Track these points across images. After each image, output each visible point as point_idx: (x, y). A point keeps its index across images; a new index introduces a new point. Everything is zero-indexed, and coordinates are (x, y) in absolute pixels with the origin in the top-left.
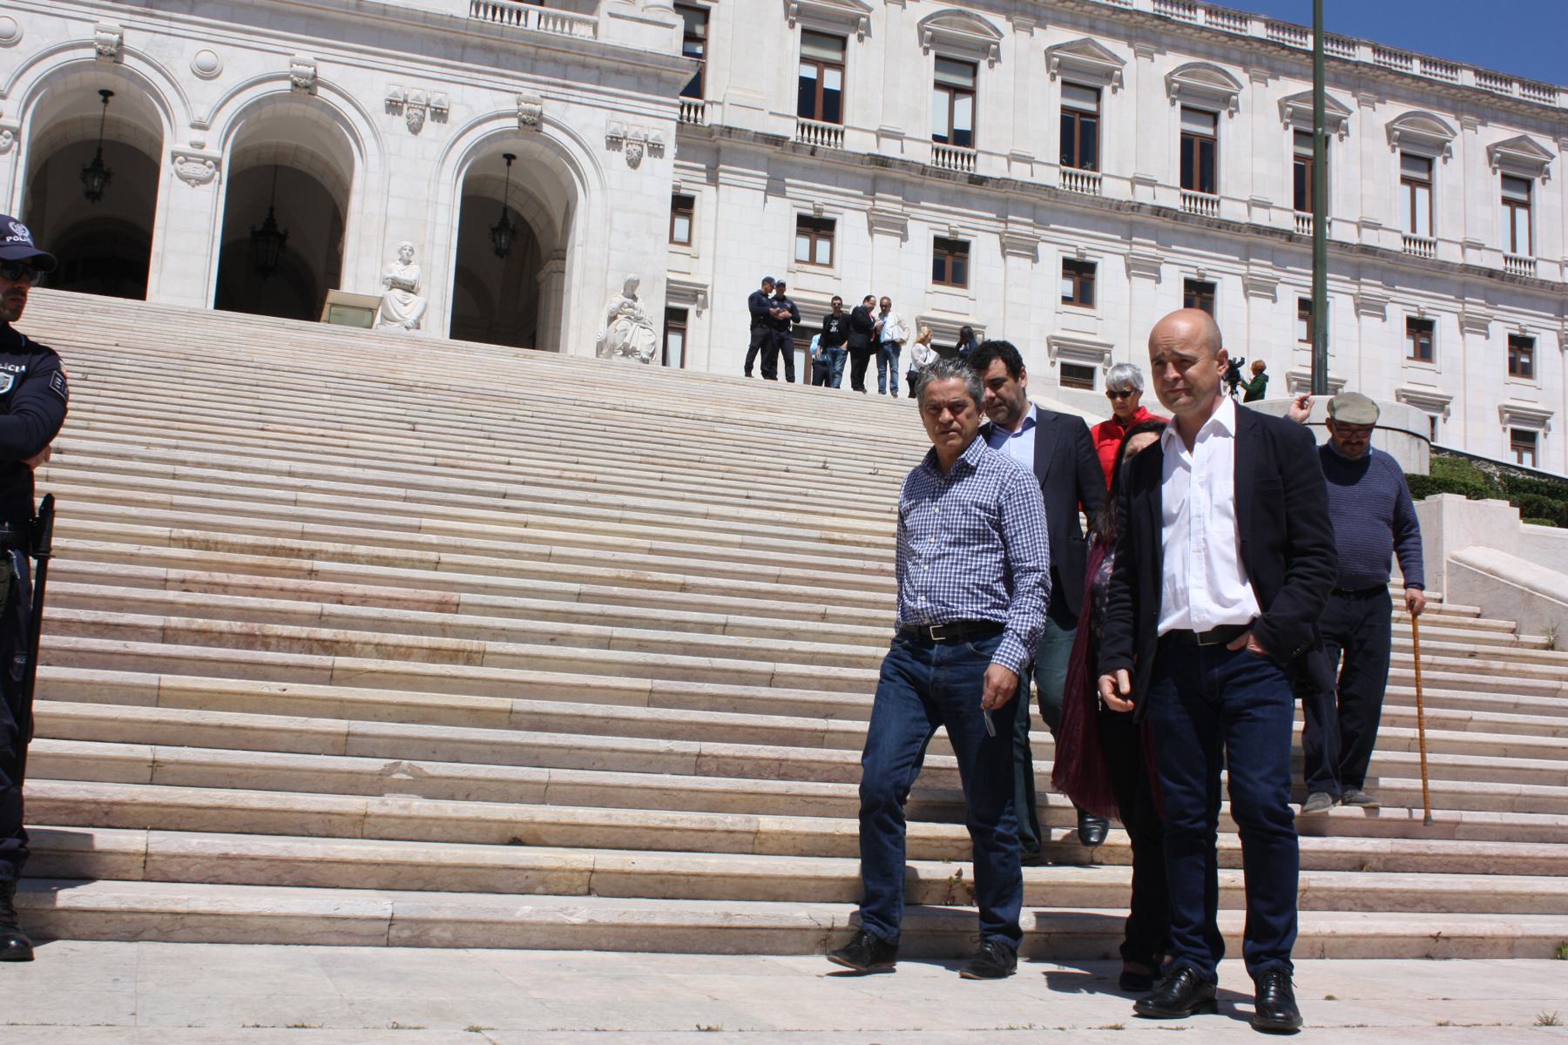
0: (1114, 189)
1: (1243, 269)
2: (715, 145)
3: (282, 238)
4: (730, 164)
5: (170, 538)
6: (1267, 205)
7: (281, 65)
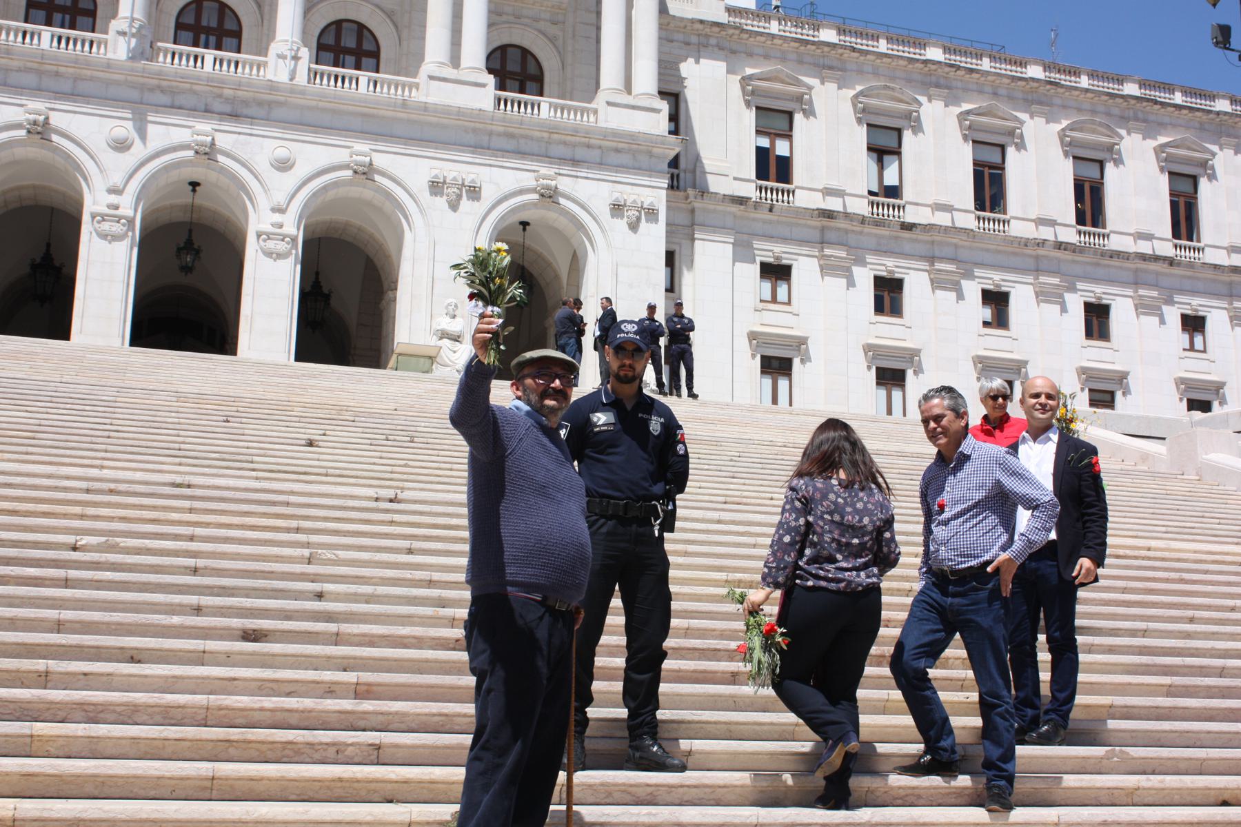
0: (1019, 229)
3: (327, 297)
5: (727, 581)
7: (342, 156)
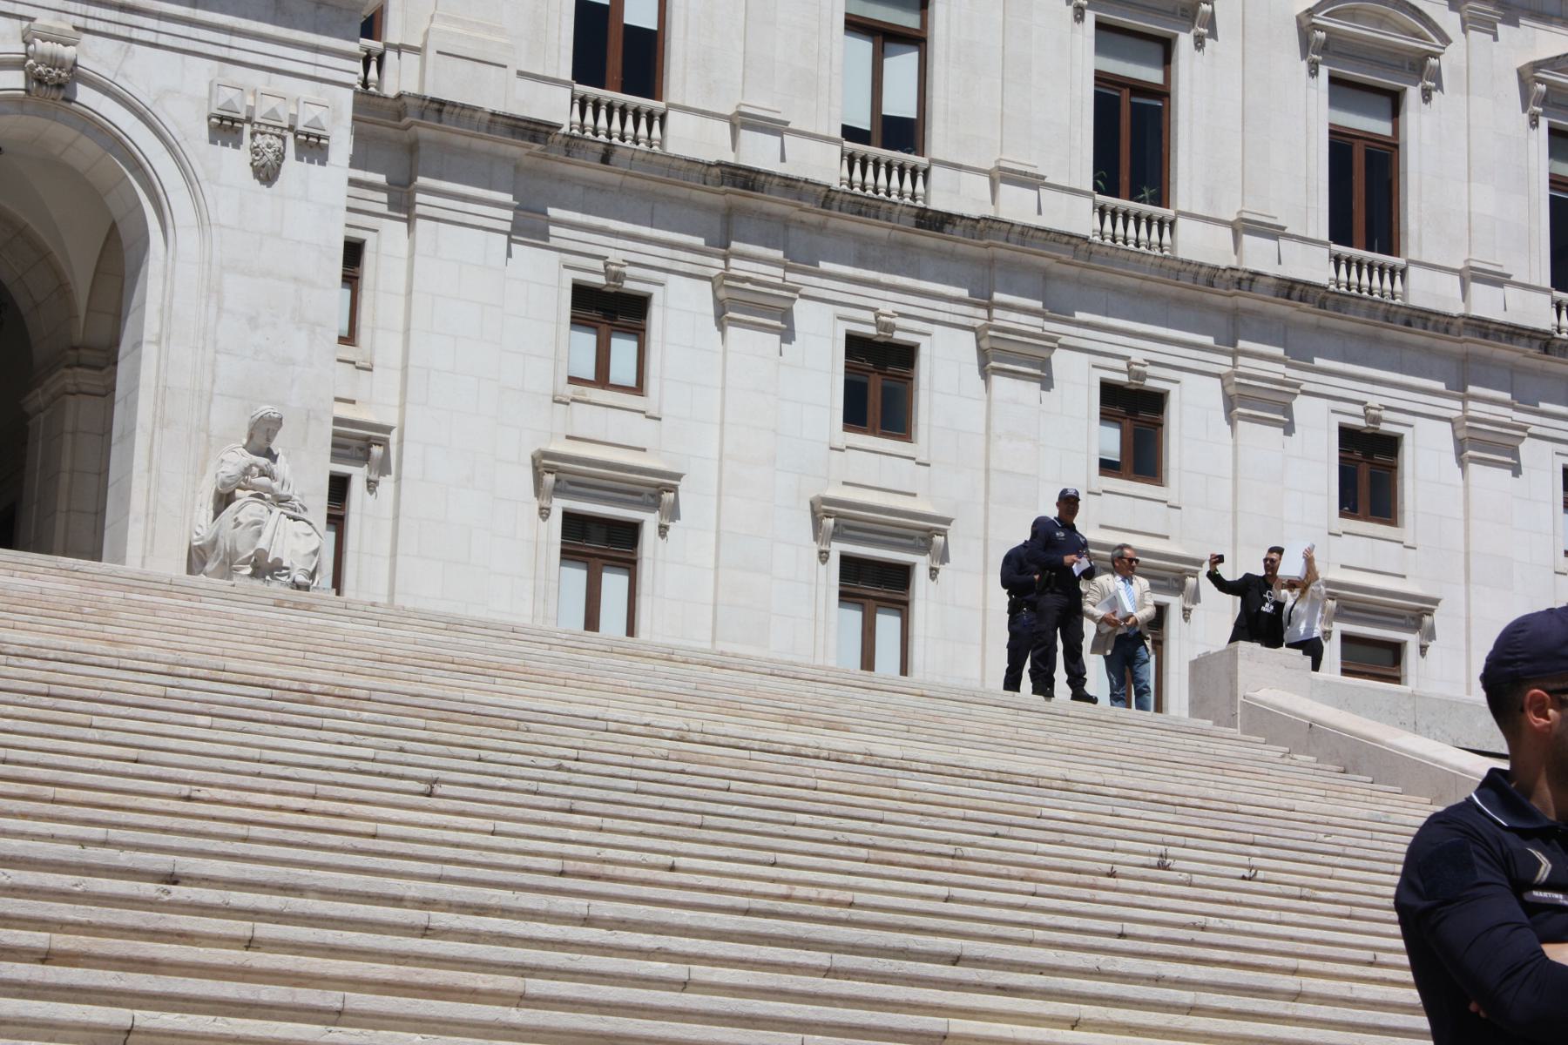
1: (1453, 407)
2: (406, 137)
4: (439, 176)
6: (1498, 280)
